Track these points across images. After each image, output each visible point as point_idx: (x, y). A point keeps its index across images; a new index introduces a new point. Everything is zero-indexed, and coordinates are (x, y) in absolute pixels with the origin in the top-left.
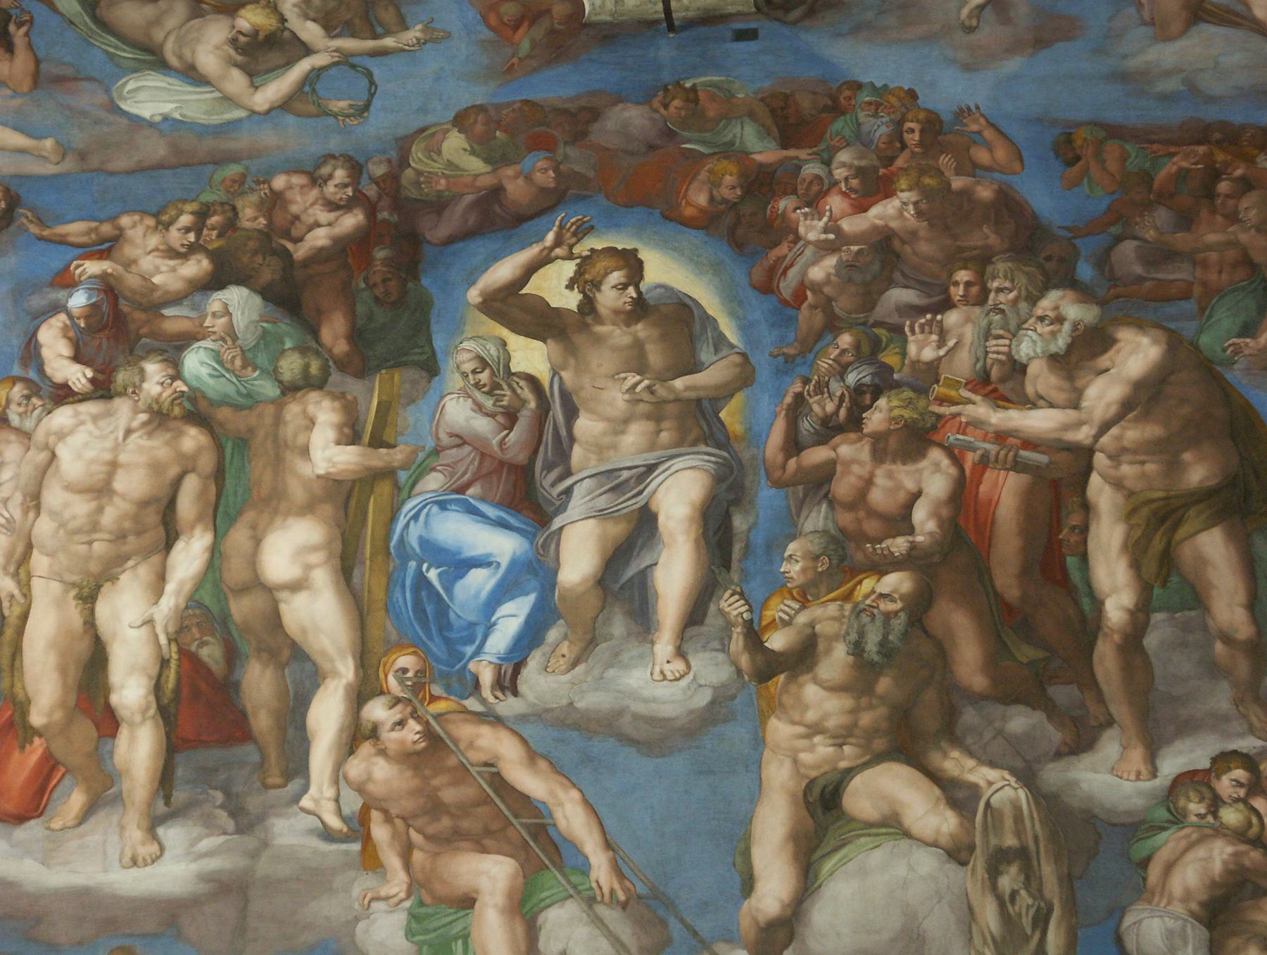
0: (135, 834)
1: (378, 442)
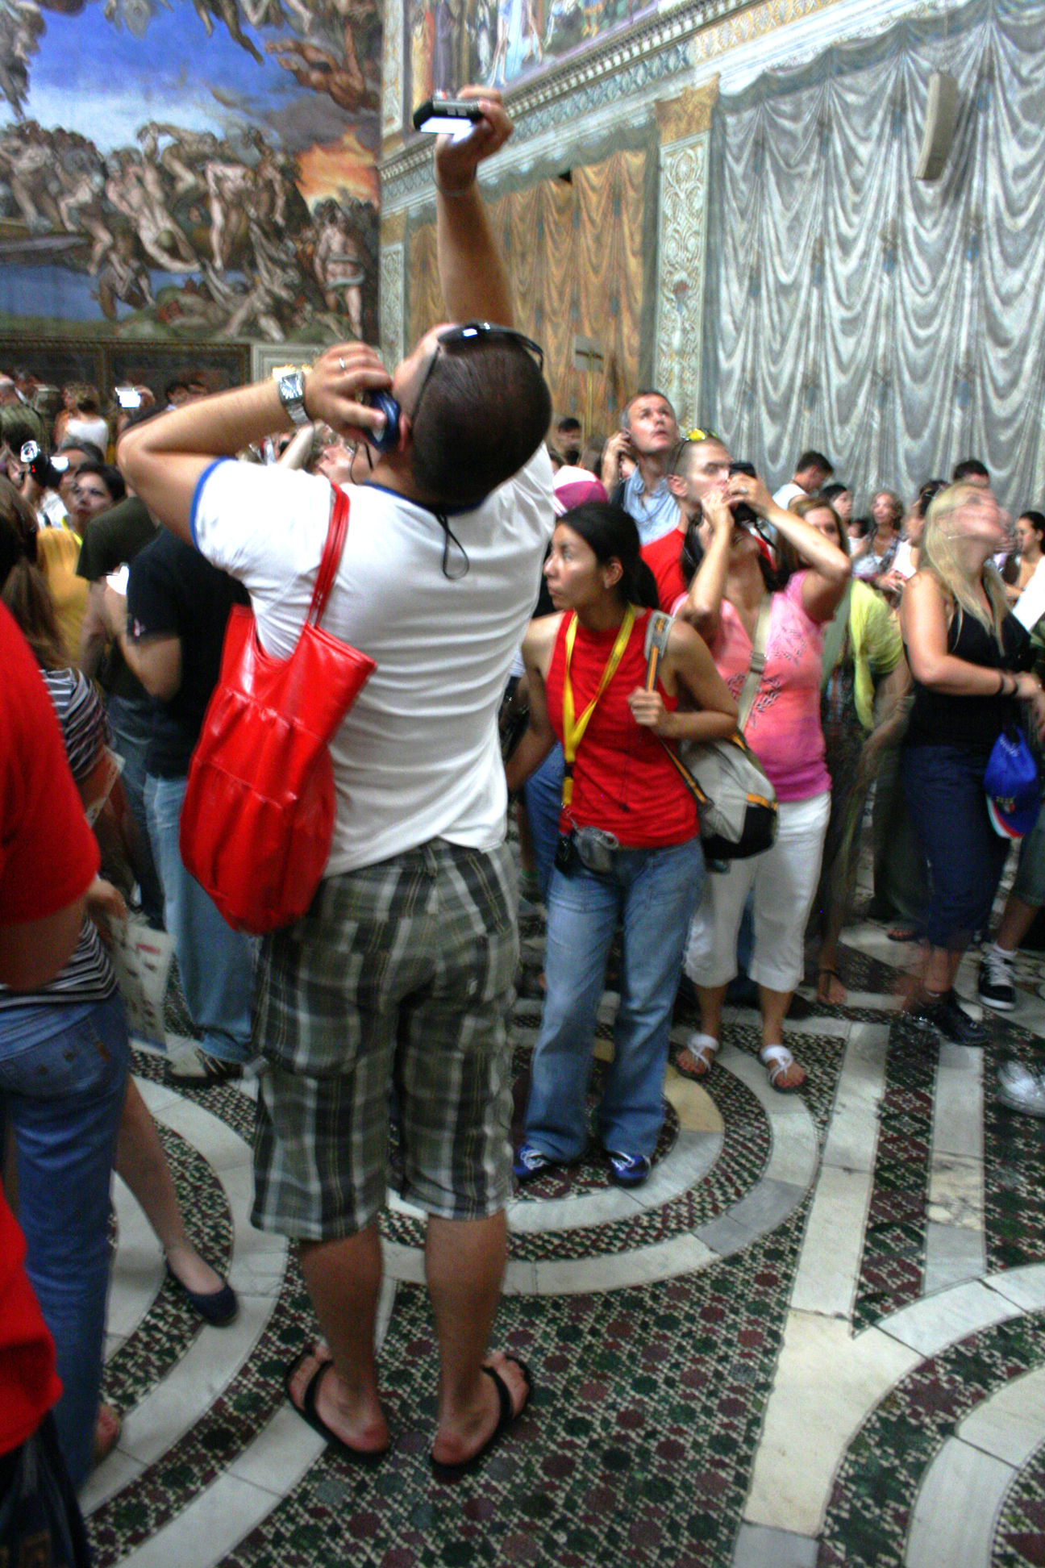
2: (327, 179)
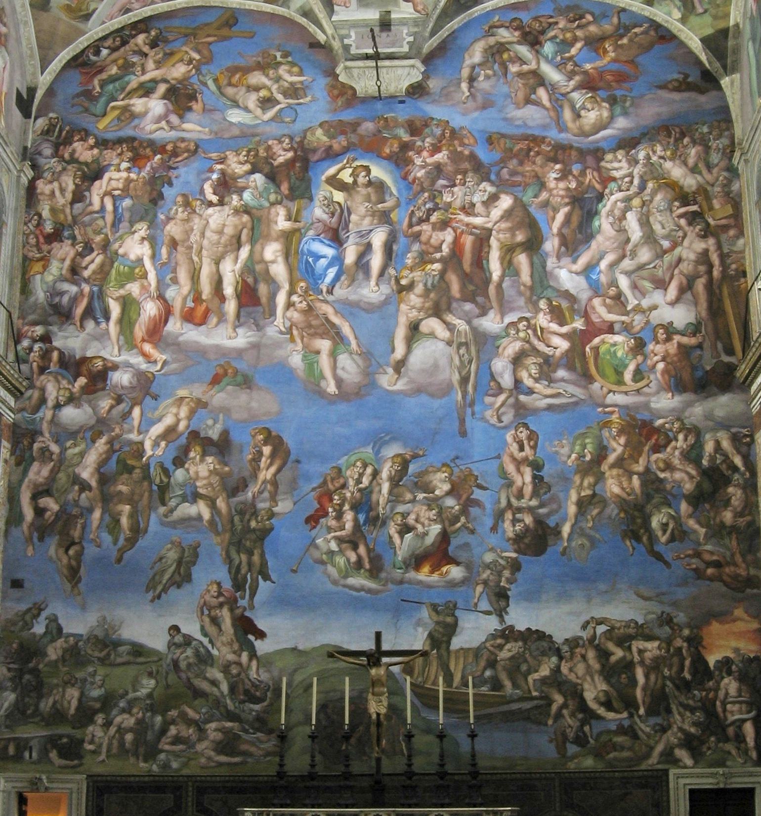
0: (230, 330)
1: (296, 221)
2: (722, 642)
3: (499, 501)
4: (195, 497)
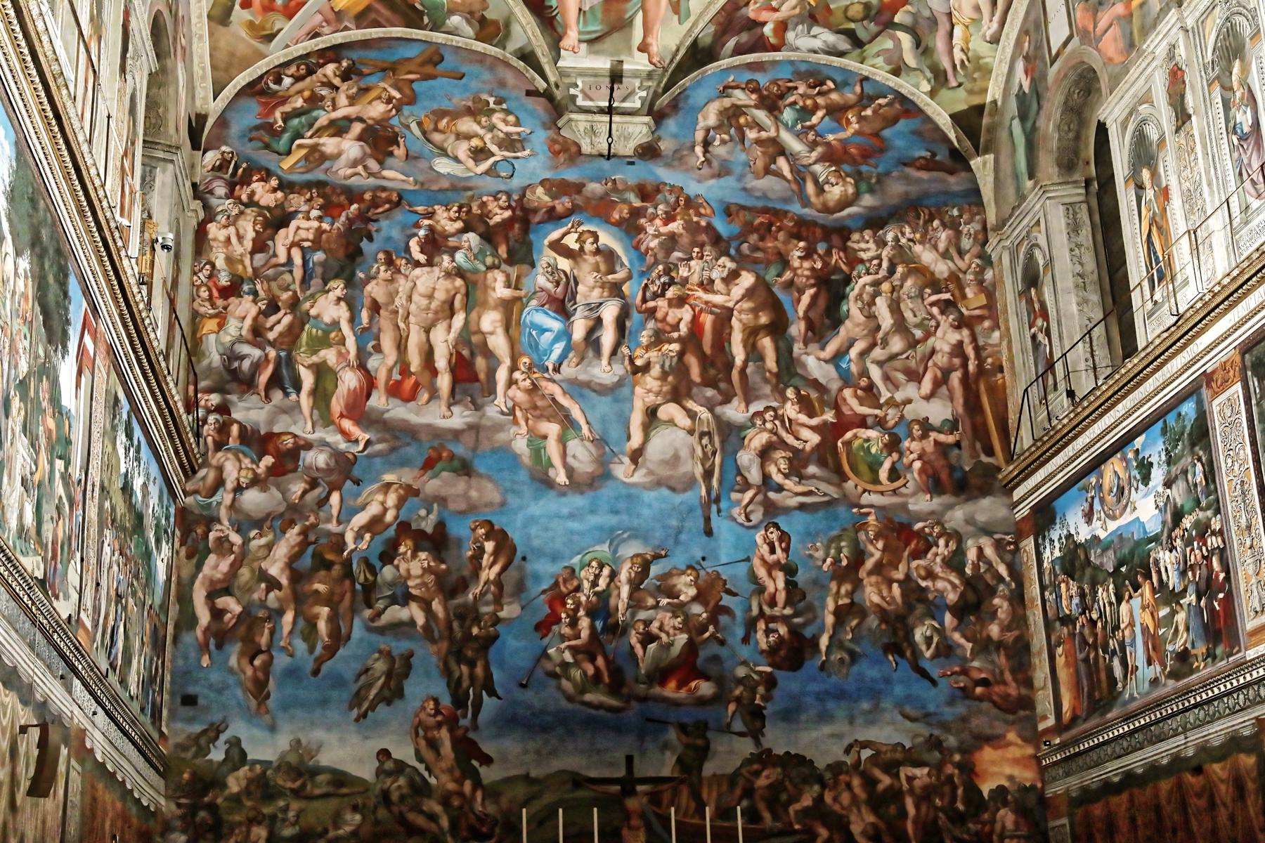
0: (444, 408)
1: (517, 288)
2: (995, 769)
3: (750, 609)
4: (405, 598)
